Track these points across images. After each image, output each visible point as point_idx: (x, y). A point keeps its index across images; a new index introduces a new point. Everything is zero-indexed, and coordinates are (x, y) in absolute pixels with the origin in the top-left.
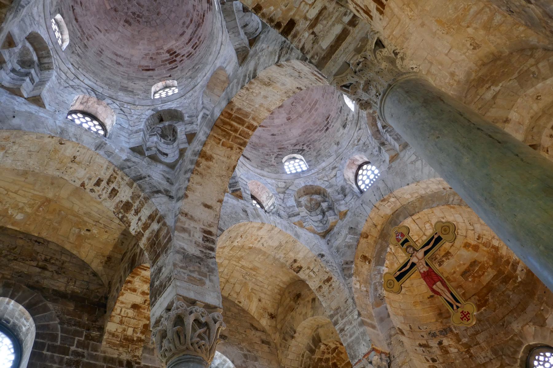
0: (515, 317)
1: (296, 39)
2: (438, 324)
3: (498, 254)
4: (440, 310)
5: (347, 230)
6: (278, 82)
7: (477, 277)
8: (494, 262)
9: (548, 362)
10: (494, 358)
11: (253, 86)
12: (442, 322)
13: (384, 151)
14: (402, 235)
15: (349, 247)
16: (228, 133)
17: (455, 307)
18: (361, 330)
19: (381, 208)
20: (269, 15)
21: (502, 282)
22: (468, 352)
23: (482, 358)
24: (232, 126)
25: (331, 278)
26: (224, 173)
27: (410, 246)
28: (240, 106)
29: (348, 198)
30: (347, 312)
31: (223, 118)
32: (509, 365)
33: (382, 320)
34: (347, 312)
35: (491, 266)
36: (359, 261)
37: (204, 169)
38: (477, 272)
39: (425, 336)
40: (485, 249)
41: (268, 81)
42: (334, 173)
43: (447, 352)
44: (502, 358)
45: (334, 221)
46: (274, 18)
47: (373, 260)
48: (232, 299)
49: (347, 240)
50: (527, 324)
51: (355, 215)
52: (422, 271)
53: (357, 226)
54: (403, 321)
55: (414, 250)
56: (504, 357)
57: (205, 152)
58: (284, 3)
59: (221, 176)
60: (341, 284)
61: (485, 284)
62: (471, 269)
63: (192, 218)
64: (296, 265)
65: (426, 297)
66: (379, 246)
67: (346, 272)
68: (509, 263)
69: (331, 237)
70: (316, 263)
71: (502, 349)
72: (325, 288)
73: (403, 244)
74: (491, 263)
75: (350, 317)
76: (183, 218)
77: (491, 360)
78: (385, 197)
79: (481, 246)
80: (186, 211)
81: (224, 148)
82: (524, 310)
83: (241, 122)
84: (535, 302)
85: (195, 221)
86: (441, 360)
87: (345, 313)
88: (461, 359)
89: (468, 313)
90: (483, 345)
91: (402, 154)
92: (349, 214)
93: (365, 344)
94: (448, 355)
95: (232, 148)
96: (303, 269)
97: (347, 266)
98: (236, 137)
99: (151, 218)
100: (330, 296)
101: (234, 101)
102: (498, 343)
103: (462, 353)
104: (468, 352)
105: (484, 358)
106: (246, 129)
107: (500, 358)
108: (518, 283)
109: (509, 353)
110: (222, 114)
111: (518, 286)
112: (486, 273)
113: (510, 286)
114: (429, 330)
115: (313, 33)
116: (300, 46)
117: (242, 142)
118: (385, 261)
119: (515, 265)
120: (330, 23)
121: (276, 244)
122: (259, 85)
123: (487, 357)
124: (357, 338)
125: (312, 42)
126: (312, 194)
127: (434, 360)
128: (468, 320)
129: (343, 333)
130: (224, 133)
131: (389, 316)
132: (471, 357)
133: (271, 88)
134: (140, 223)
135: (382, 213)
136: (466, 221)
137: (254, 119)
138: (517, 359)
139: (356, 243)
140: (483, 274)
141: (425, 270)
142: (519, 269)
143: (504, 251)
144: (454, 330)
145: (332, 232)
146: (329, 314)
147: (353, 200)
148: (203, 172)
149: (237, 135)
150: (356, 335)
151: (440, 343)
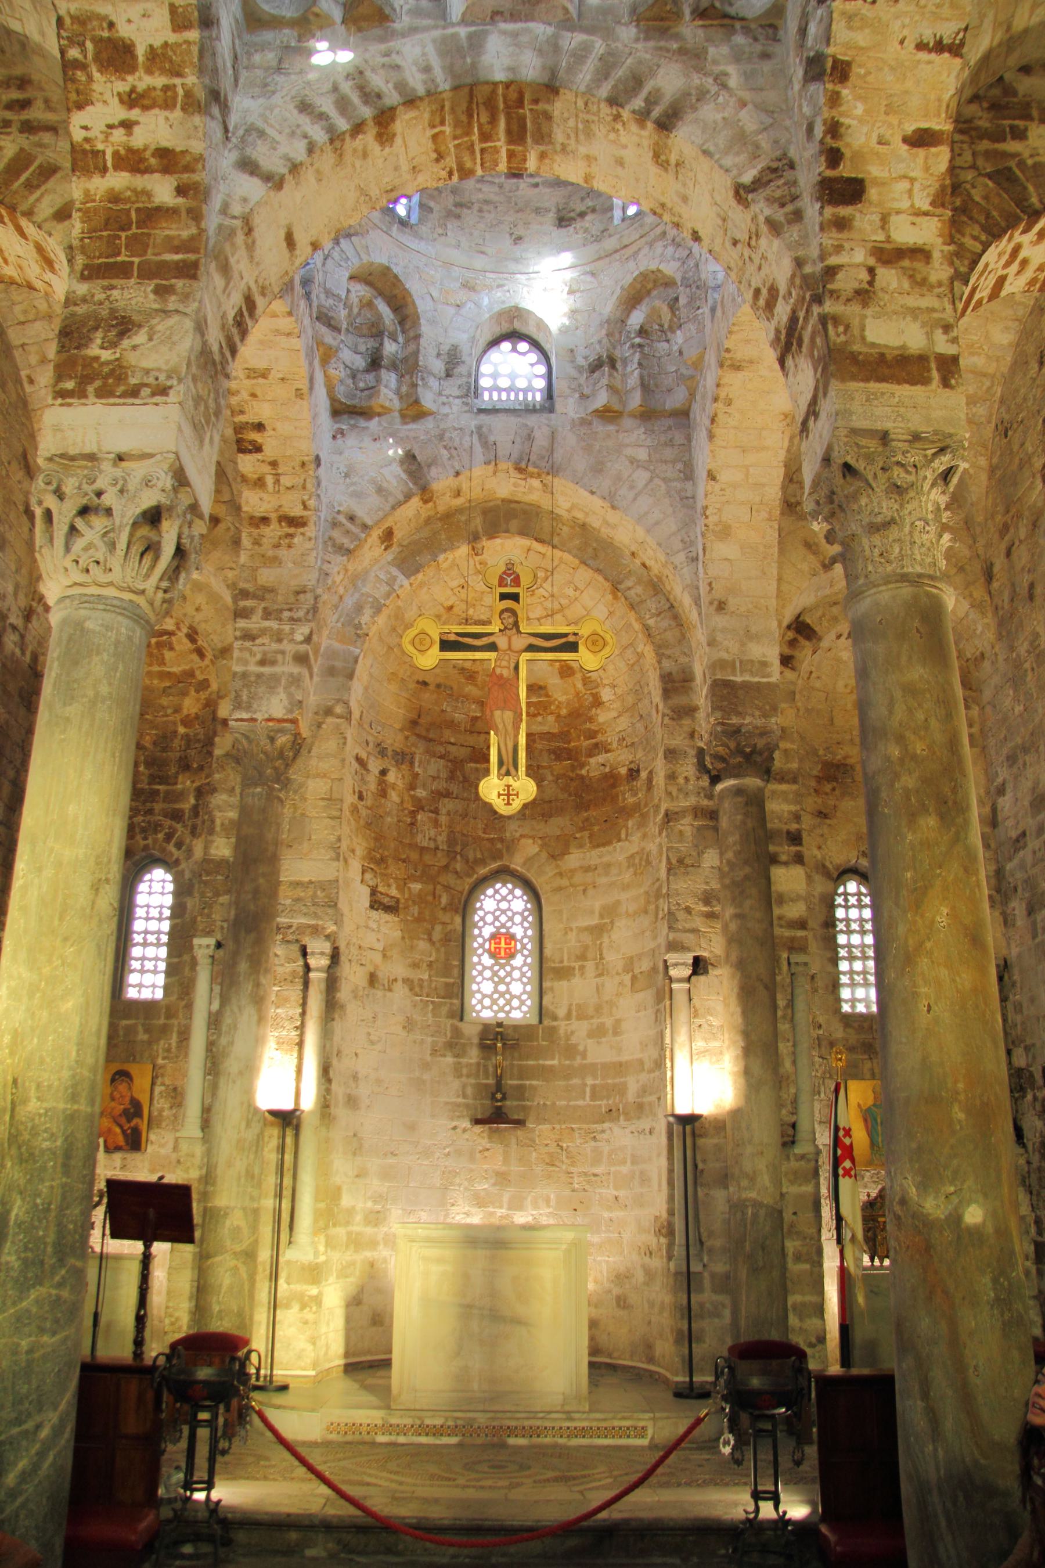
1: (834, 233)
2: (400, 737)
3: (590, 709)
6: (684, 185)
8: (570, 715)
11: (634, 128)
13: (605, 381)
14: (517, 582)
16: (470, 124)
17: (504, 770)
18: (296, 670)
20: (841, 115)
21: (550, 752)
22: (413, 814)
24: (493, 121)
25: (304, 524)
26: (375, 192)
27: (514, 613)
28: (556, 113)
29: (452, 388)
30: (286, 614)
31: (500, 91)
33: (331, 671)
34: (286, 614)
35: (559, 716)
36: (376, 533)
37: (355, 151)
40: (579, 685)
41: (673, 162)
42: (462, 296)
43: (383, 793)
45: (387, 404)
46: (842, 130)
47: (395, 549)
48: (18, 360)
49: (386, 471)
50: (533, 837)
51: (441, 437)
52: (498, 671)
55: (516, 624)
57: (393, 119)
58: (882, 131)
59: (363, 192)
63: (250, 247)
64: (254, 436)
65: (416, 678)
69: (354, 427)
71: (465, 845)
72: (273, 532)
73: (503, 597)
74: (564, 712)
76: (240, 238)
78: (530, 469)
79: (579, 676)
80: (257, 221)
81: (430, 145)
82: (546, 816)
83: (517, 135)
85: (251, 258)
86: (369, 803)
87: (281, 611)
90: (443, 819)
91: (627, 422)
92: (429, 423)
93: (286, 702)
95: (440, 157)
96: (259, 456)
97: (349, 525)
98: (471, 148)
99: (168, 160)
100: (270, 553)
101: (562, 97)
104: (413, 814)
106: (504, 154)
109: (471, 857)
110: (507, 85)
112: (539, 719)
113: (559, 767)
115: (871, 271)
116: (833, 261)
117: (468, 165)
118: (417, 571)
119: (598, 748)
120: (912, 301)
121: (261, 364)
122: (645, 143)
124: (275, 679)
125: (856, 285)
126: (381, 294)
127: (361, 798)
129: (248, 644)
130: (464, 118)
131: (351, 676)
133: (654, 169)
134: (119, 135)
135: (492, 483)
137: (542, 156)
139: (401, 498)
141: (505, 673)
142: (601, 758)
143: (603, 717)
145: (362, 423)
146: (242, 585)
147: (458, 401)
148: (348, 158)
149: (477, 148)
150: (277, 669)
151: (384, 772)
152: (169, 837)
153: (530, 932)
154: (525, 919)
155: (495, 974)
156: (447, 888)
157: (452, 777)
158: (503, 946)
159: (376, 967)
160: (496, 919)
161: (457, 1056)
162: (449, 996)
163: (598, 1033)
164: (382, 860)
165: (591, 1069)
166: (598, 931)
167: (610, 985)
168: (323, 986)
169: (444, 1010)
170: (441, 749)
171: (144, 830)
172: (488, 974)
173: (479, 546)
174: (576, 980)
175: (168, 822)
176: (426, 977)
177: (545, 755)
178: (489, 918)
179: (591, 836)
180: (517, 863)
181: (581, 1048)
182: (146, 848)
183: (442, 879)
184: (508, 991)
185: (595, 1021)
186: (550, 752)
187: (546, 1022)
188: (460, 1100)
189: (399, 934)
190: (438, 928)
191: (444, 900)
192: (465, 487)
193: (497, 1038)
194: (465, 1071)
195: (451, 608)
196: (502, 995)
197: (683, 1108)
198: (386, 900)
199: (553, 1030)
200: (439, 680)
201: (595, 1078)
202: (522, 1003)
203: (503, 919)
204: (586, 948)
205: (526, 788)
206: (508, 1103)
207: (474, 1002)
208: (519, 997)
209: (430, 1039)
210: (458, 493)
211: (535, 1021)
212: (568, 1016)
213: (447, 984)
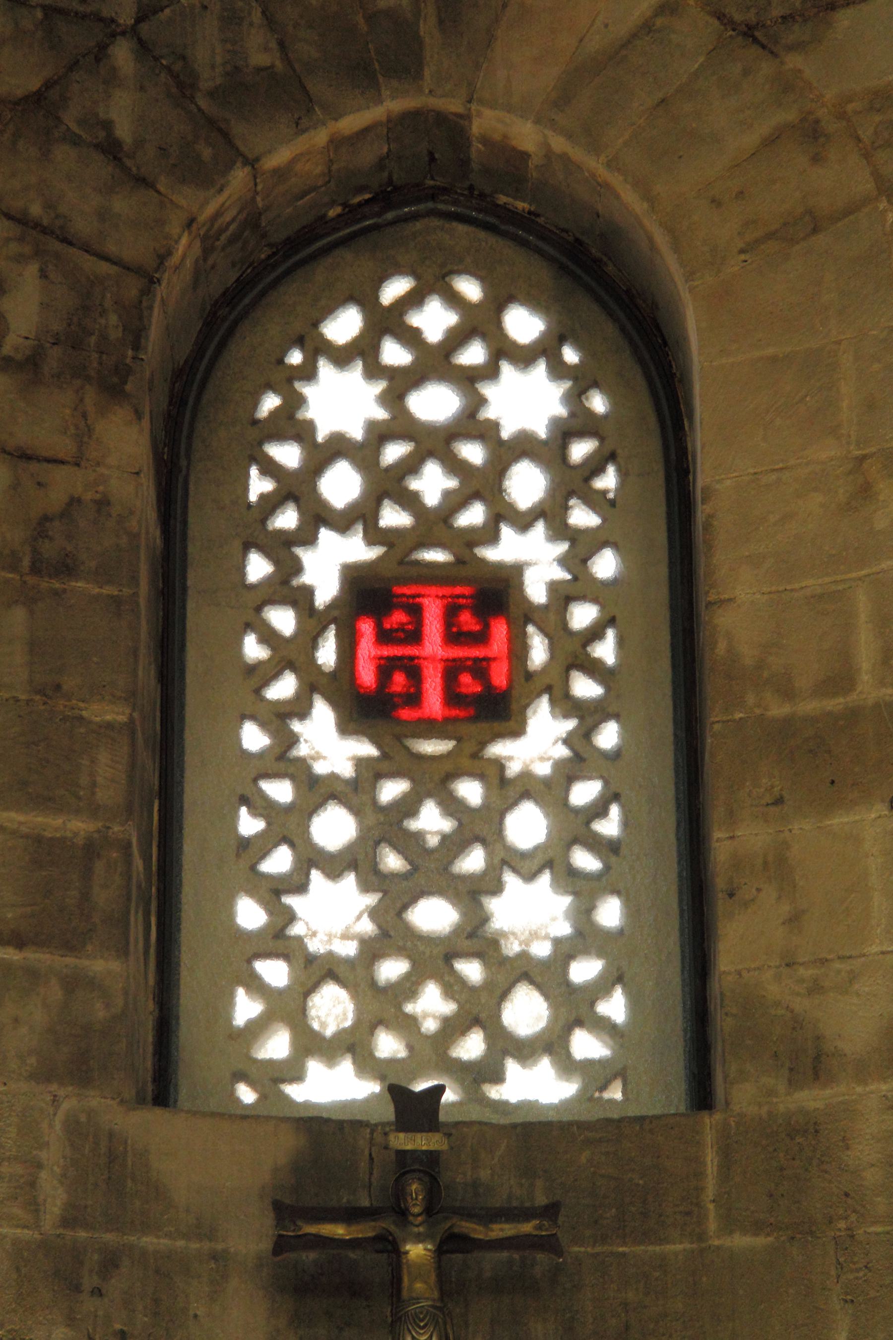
9: (469, 381)
44: (100, 53)
56: (122, 54)
109: (207, 54)
138: (233, 154)
154: (570, 484)
160: (388, 485)
162: (55, 927)
178: (341, 485)
180: (513, 120)
187: (747, 1093)
196: (434, 959)
199: (803, 1144)
202: (574, 1008)
203: (432, 483)
207: (246, 1008)
208: (547, 975)
211: (667, 1096)
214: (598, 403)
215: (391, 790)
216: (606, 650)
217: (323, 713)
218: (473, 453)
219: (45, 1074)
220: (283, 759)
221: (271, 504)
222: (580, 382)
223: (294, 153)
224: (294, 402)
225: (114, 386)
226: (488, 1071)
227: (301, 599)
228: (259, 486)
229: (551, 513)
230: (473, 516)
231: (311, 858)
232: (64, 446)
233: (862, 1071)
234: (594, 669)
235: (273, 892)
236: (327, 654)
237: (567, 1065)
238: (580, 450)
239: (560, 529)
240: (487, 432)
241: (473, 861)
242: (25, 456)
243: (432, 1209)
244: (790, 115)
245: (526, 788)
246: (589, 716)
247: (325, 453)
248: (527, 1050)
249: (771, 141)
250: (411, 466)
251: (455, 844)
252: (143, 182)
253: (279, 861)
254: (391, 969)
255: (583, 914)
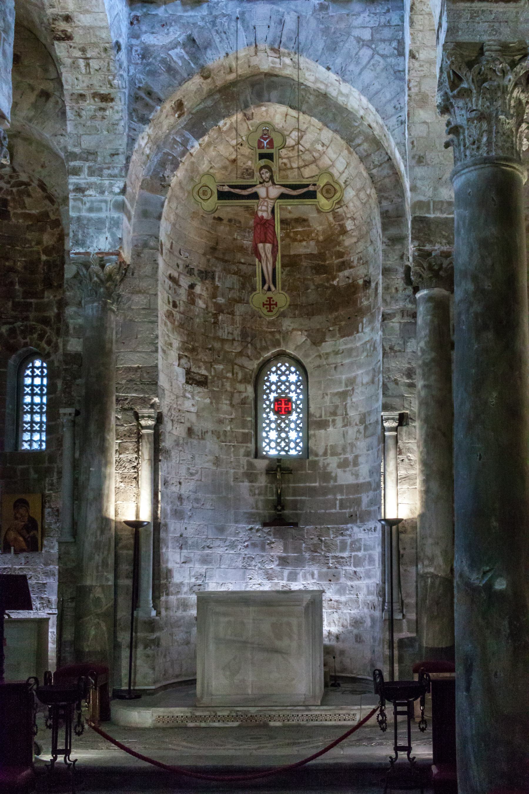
0: (295, 314)
4: (217, 243)
5: (183, 36)
7: (290, 237)
9: (287, 375)
10: (238, 341)
12: (208, 260)
15: (170, 70)
19: (261, 55)
21: (312, 268)
22: (215, 316)
23: (226, 332)
32: (248, 357)
38: (296, 233)
39: (181, 267)
44: (247, 345)
50: (301, 330)
53: (206, 48)
54: (169, 233)
56: (249, 345)
60: (122, 123)
61: (292, 253)
62: (293, 223)
66: (209, 103)
67: (138, 106)
68: (342, 257)
70: (103, 55)
71: (254, 337)
75: (107, 182)
77: (234, 340)
82: (310, 314)
84: (330, 316)
88: (202, 320)
89: (276, 304)
90: (238, 318)
94: (192, 307)
102: (254, 328)
103: (207, 314)
105: (228, 333)
107: (245, 344)
108: (331, 285)
109: (258, 346)
111: (327, 288)
114: (188, 261)
123: (232, 334)
128: (270, 311)
132: (215, 323)
135: (255, 61)
136: (344, 175)
138: (261, 356)
140: (301, 241)
144: (217, 279)
152: (41, 337)
153: (301, 397)
154: (298, 387)
155: (279, 425)
156: (242, 367)
157: (243, 287)
158: (283, 406)
159: (192, 423)
160: (278, 387)
161: (251, 481)
163: (343, 465)
164: (193, 350)
165: (340, 489)
166: (344, 395)
167: (352, 432)
168: (152, 439)
169: (242, 451)
170: (234, 268)
171: (22, 332)
172: (273, 426)
173: (249, 113)
174: (330, 429)
175: (39, 326)
176: (229, 428)
177: (309, 270)
178: (274, 387)
179: (339, 330)
181: (333, 475)
182: (26, 345)
183: (239, 361)
184: (287, 437)
185: (342, 456)
186: (312, 268)
188: (254, 511)
189: (208, 401)
190: (236, 395)
191: (240, 376)
192: (234, 64)
193: (279, 469)
194: (257, 492)
195: (234, 161)
196: (283, 439)
197: (391, 515)
198: (197, 377)
200: (231, 216)
201: (342, 494)
202: (297, 444)
203: (283, 387)
204: (337, 407)
205: (282, 299)
206: (286, 512)
207: (264, 444)
209: (232, 471)
210: (231, 71)
212: (325, 454)
213: (244, 434)
214: (301, 378)
215: (279, 421)
216: (301, 406)
217: (272, 413)
218: (287, 384)
219: (244, 456)
220: (268, 418)
221: (266, 389)
222: (299, 376)
223: (267, 355)
224: (269, 378)
225: (249, 382)
226: (288, 451)
227: (269, 400)
228: (265, 387)
229: (295, 391)
230: (287, 391)
231: (271, 429)
232: (244, 390)
233: (321, 456)
234: (300, 408)
235: (267, 432)
236: (272, 406)
237: (296, 450)
238: (299, 383)
239: (296, 393)
240: (289, 381)
241: (287, 429)
242: (240, 392)
243: (281, 470)
244: (317, 354)
245: (293, 421)
246: (299, 413)
247: (272, 384)
248: (292, 449)
249: (316, 356)
250: (281, 385)
251: (285, 427)
252: (252, 360)
253: (267, 429)
254: (279, 440)
255: (298, 435)
